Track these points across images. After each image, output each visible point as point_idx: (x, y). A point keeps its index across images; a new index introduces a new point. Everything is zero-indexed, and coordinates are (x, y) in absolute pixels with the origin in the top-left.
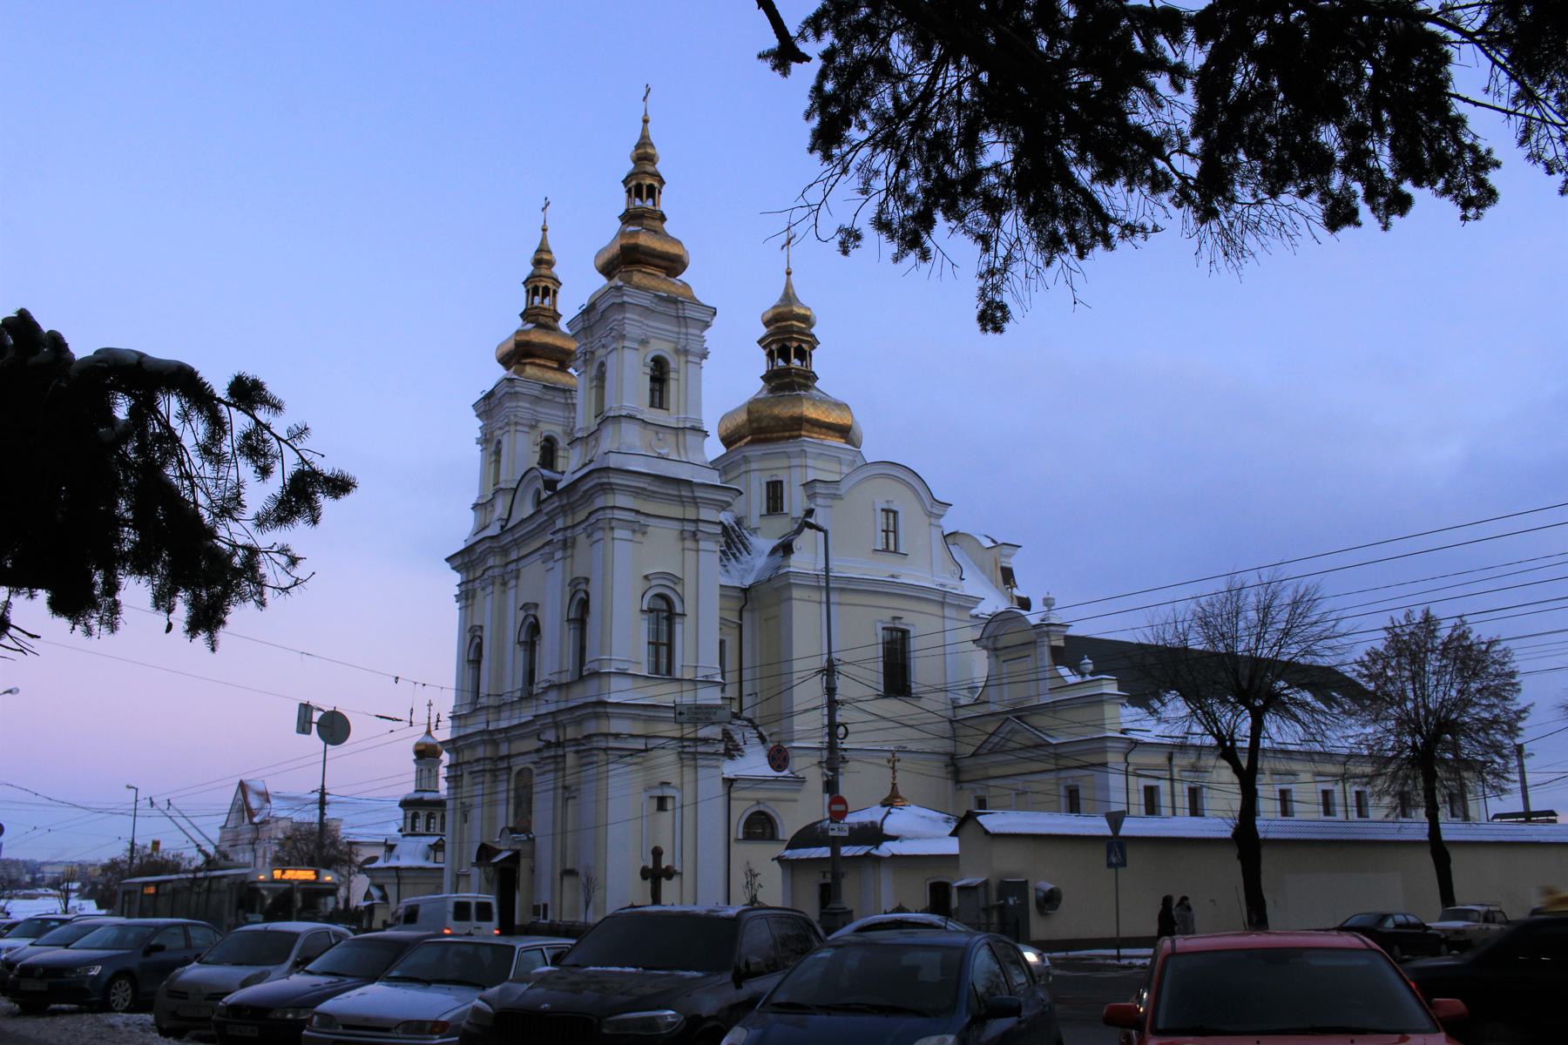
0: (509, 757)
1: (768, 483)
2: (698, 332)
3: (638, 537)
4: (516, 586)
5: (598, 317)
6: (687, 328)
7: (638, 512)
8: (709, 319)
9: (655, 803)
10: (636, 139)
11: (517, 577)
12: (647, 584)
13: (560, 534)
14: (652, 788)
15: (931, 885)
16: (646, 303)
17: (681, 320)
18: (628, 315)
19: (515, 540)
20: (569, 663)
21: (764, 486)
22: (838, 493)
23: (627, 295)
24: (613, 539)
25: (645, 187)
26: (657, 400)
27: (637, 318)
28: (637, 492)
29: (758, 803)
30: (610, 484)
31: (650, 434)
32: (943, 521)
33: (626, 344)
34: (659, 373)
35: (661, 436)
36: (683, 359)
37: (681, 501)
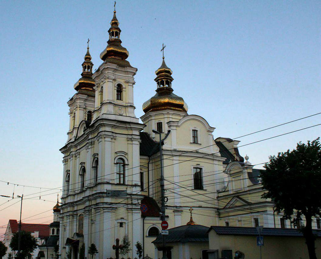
0: (77, 210)
1: (157, 123)
3: (113, 140)
5: (100, 73)
7: (113, 132)
8: (135, 72)
9: (119, 224)
10: (112, 18)
11: (79, 155)
12: (116, 155)
13: (90, 140)
14: (118, 219)
15: (203, 251)
20: (93, 181)
21: (156, 125)
22: (178, 125)
27: (112, 72)
28: (113, 126)
29: (153, 224)
30: (104, 124)
32: (213, 133)
34: (120, 89)
36: (127, 84)
37: (127, 128)
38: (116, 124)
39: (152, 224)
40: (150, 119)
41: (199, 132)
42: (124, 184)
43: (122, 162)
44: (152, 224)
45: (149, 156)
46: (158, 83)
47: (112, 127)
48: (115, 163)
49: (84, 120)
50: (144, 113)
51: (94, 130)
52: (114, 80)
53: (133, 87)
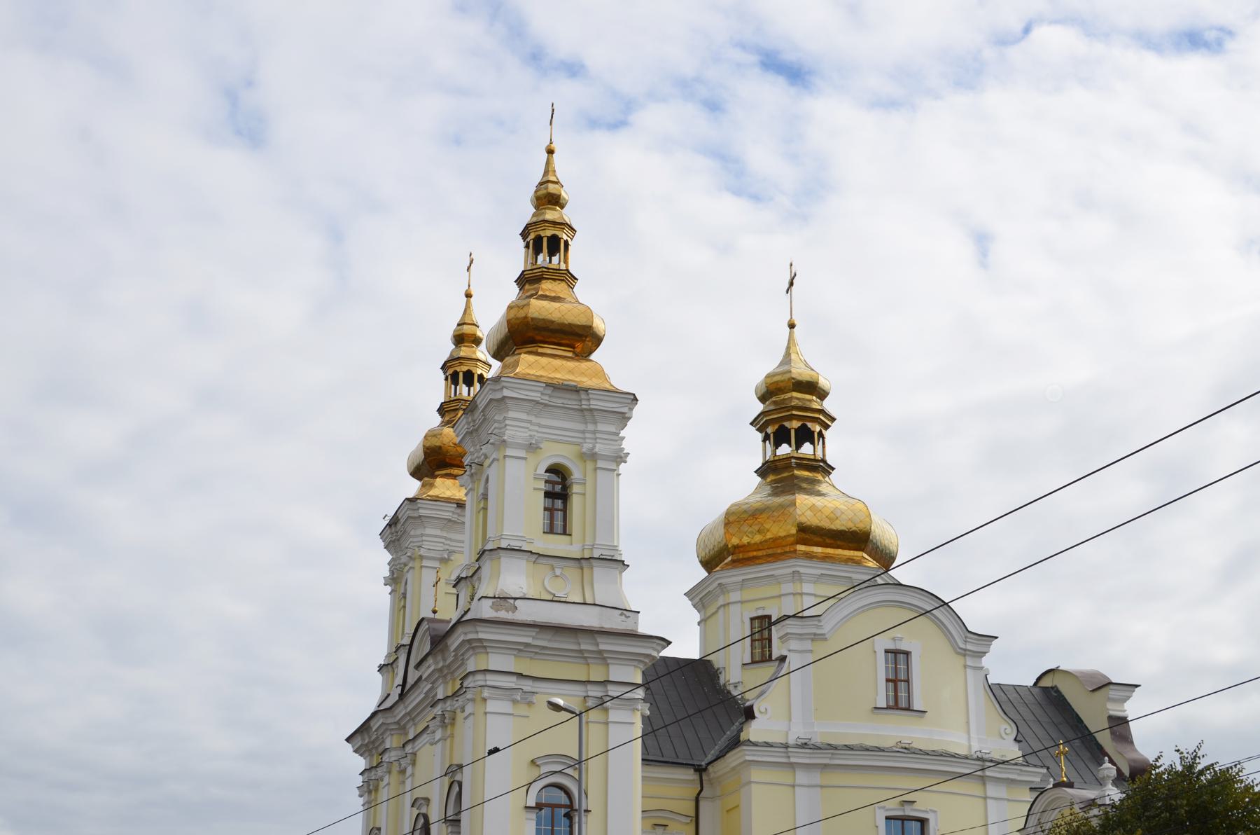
1: (752, 619)
2: (612, 429)
3: (522, 710)
4: (412, 775)
6: (595, 423)
7: (520, 675)
8: (625, 410)
10: (538, 178)
11: (414, 763)
12: (535, 773)
16: (536, 396)
17: (586, 413)
18: (511, 414)
19: (409, 714)
22: (819, 632)
23: (506, 388)
24: (486, 713)
25: (545, 240)
26: (559, 523)
27: (524, 416)
28: (521, 650)
30: (480, 640)
31: (543, 568)
32: (986, 661)
33: (509, 452)
35: (558, 572)
36: (590, 465)
37: (582, 656)
38: (534, 638)
40: (721, 601)
41: (915, 659)
43: (563, 799)
45: (700, 770)
47: (515, 653)
48: (526, 807)
49: (431, 615)
50: (703, 574)
51: (452, 662)
52: (532, 447)
53: (619, 475)
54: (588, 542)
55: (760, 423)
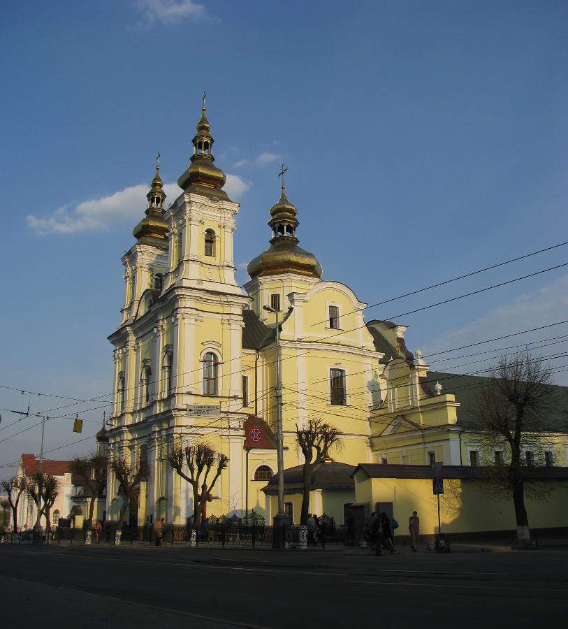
3: (199, 323)
7: (197, 310)
12: (203, 347)
21: (270, 297)
36: (223, 230)
37: (221, 303)
39: (261, 461)
42: (215, 396)
44: (261, 461)
45: (258, 350)
46: (274, 229)
54: (222, 259)
55: (272, 224)
